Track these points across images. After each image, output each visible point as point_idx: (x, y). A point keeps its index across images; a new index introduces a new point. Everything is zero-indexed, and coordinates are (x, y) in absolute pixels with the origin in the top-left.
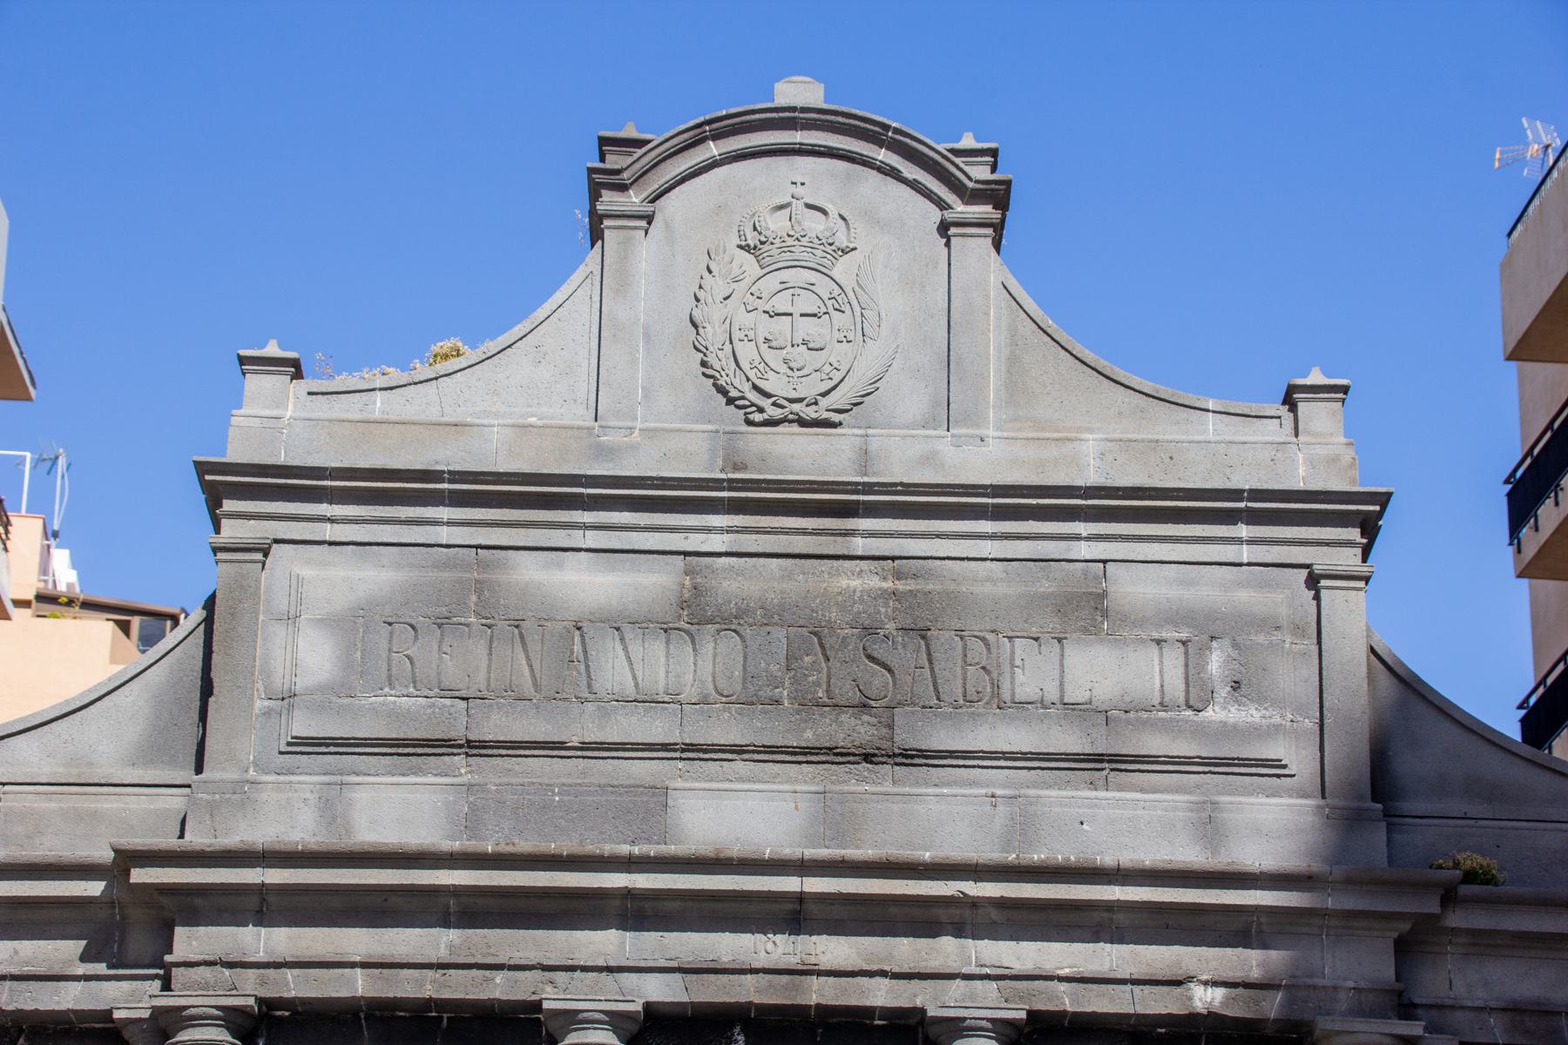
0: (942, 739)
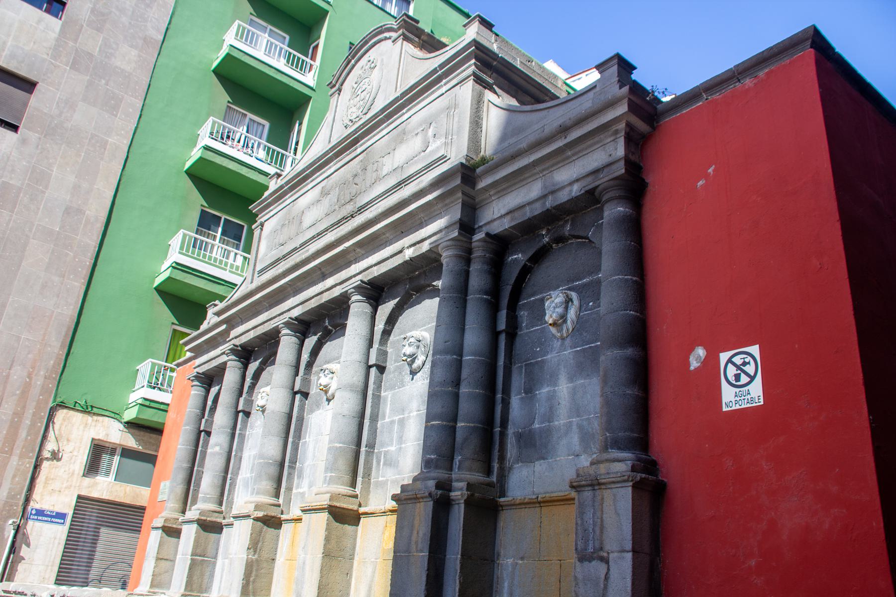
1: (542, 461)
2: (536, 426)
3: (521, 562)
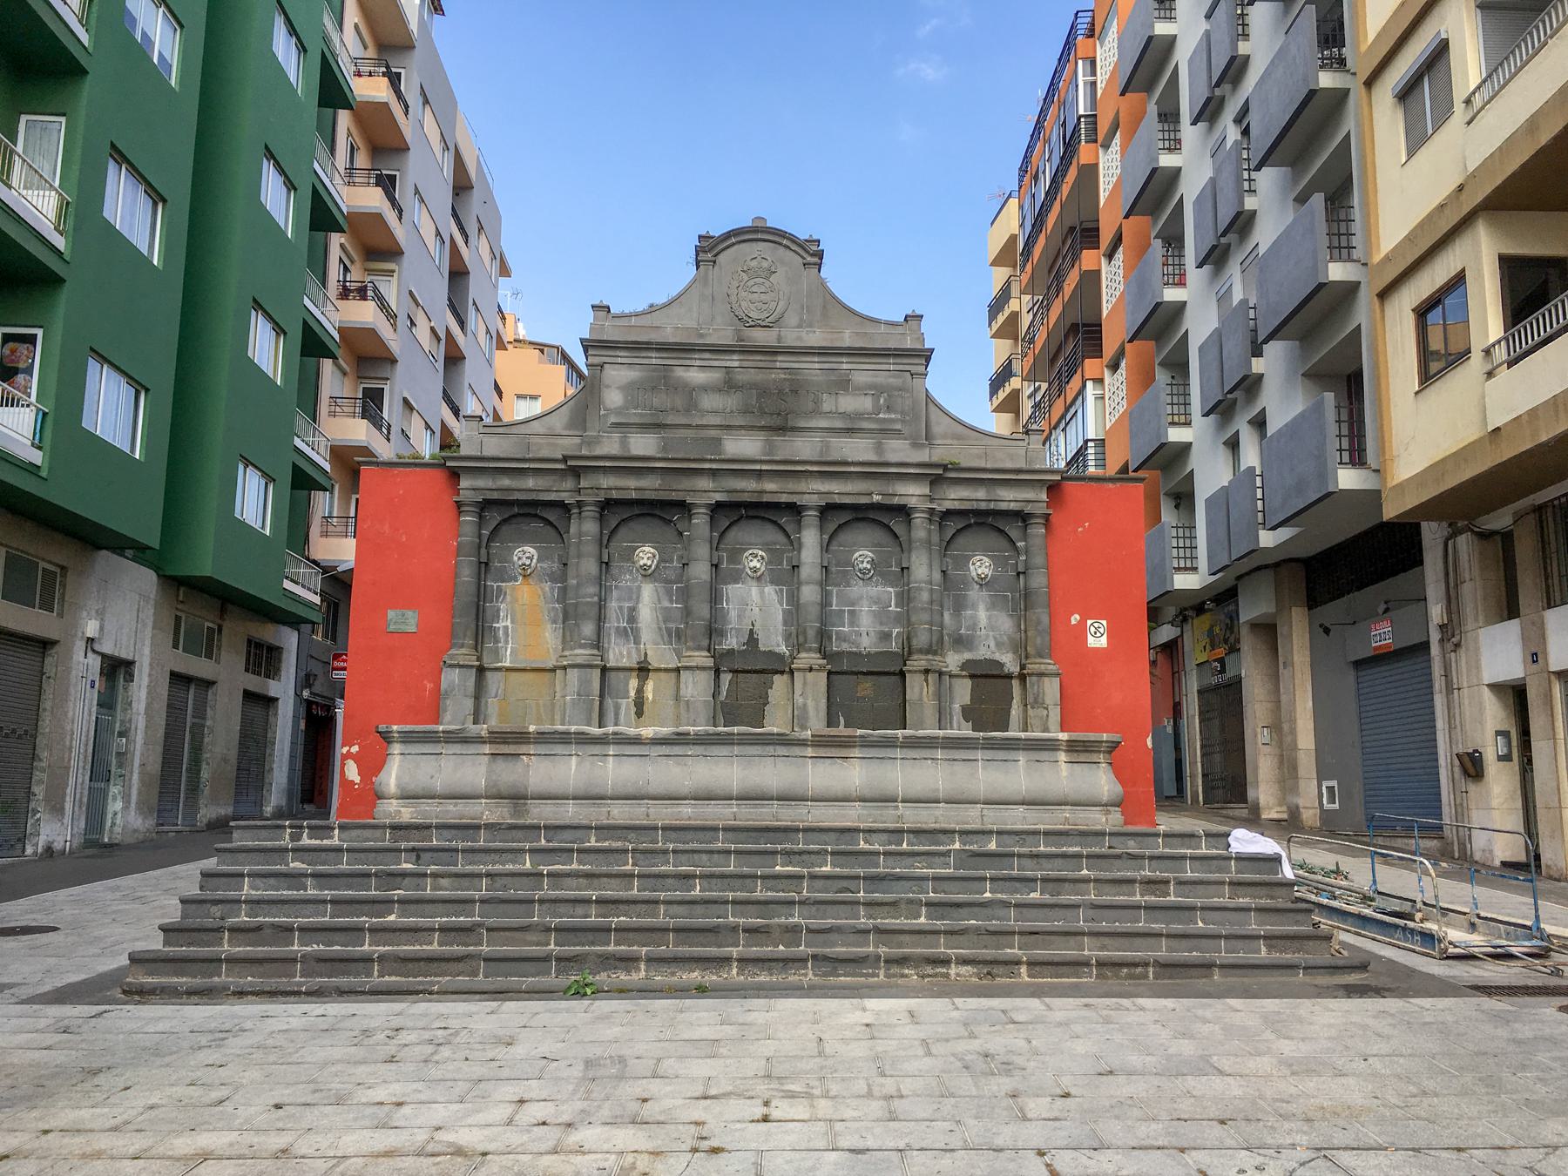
0: (802, 424)
2: (962, 631)
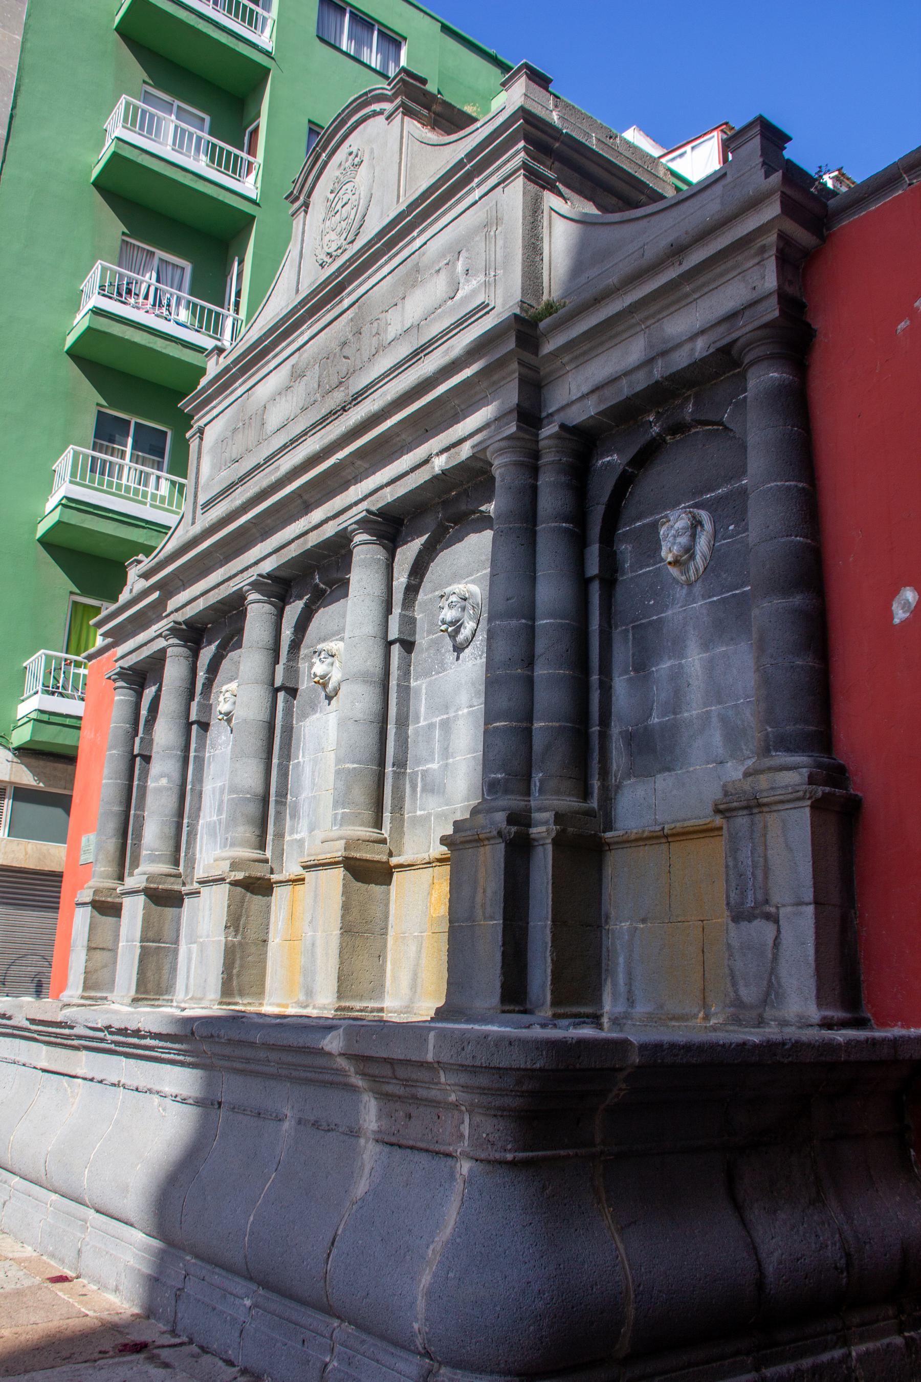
1: (667, 774)
2: (655, 720)
3: (642, 926)
